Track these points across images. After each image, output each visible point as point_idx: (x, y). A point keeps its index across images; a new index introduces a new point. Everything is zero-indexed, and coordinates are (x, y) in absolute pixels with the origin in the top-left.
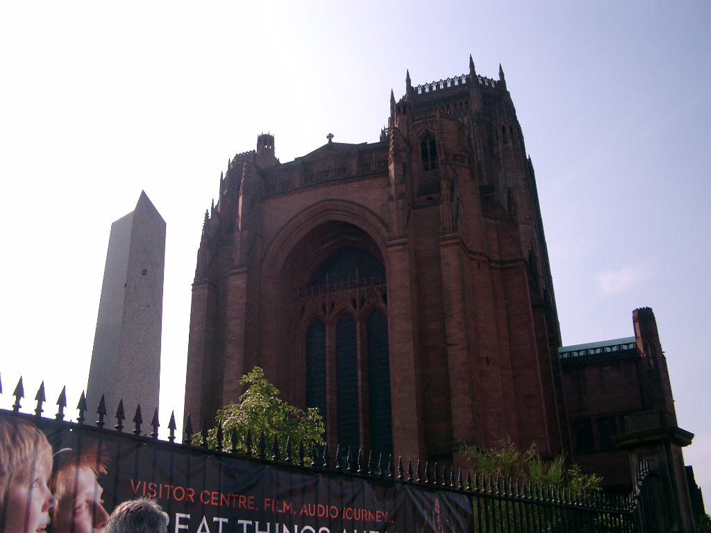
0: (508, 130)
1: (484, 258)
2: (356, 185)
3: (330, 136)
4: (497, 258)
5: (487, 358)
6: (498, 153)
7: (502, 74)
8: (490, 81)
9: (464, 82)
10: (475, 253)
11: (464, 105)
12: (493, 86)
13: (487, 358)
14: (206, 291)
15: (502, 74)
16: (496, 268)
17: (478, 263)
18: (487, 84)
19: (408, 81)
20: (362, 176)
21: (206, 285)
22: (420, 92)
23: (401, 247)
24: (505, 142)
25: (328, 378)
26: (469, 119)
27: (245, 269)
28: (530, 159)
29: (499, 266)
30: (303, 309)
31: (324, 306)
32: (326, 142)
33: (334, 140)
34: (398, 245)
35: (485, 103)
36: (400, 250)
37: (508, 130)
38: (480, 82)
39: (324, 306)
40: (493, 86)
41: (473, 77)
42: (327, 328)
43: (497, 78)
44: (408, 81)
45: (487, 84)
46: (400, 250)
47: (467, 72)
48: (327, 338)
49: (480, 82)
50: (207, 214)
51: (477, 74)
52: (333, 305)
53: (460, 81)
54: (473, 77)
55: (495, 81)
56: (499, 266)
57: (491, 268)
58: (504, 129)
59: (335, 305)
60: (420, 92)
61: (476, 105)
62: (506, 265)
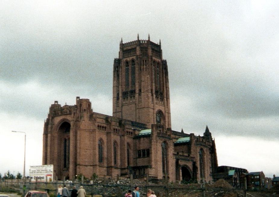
0: (145, 61)
3: (66, 103)
7: (149, 38)
8: (145, 41)
15: (149, 38)
18: (144, 42)
20: (69, 114)
24: (143, 66)
32: (65, 104)
33: (67, 104)
38: (141, 42)
40: (146, 42)
43: (147, 39)
44: (122, 41)
45: (144, 42)
51: (140, 39)
54: (139, 41)
58: (143, 61)
61: (138, 52)
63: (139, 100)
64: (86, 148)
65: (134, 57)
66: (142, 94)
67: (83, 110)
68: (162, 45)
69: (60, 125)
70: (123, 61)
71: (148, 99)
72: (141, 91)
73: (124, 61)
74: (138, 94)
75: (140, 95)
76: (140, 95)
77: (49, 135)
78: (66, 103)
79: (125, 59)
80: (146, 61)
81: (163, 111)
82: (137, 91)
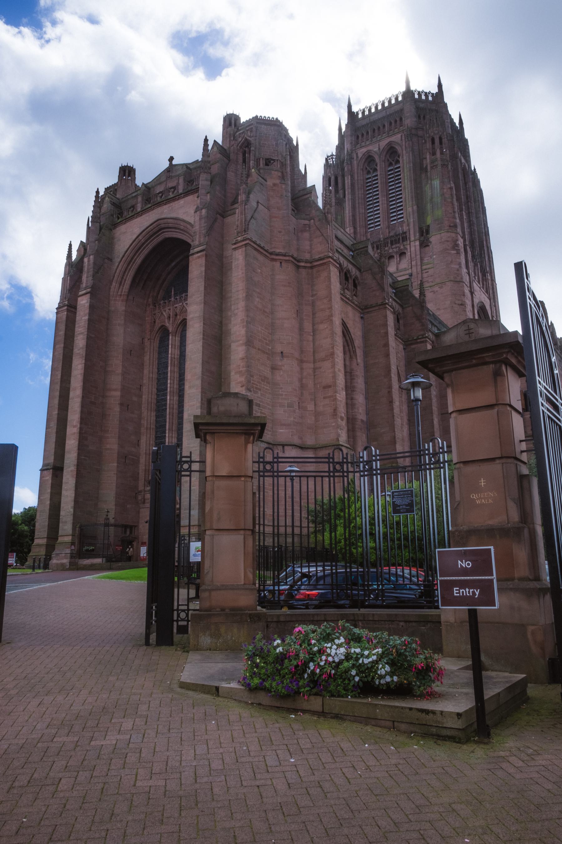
0: (437, 141)
1: (287, 258)
2: (182, 202)
3: (171, 159)
4: (307, 256)
5: (282, 352)
6: (427, 166)
7: (440, 86)
9: (400, 99)
10: (277, 255)
11: (398, 122)
12: (430, 98)
13: (282, 352)
14: (66, 313)
15: (440, 86)
16: (305, 267)
17: (281, 263)
18: (423, 97)
19: (350, 106)
20: (187, 193)
21: (66, 308)
22: (360, 116)
23: (199, 254)
24: (434, 154)
25: (169, 381)
26: (402, 136)
27: (89, 290)
28: (475, 169)
29: (309, 265)
30: (155, 322)
31: (169, 317)
32: (167, 165)
33: (174, 162)
34: (198, 252)
35: (419, 117)
36: (199, 257)
37: (437, 141)
38: (416, 96)
39: (169, 317)
40: (430, 98)
41: (408, 93)
42: (170, 337)
43: (435, 90)
44: (350, 106)
45: (423, 97)
46: (199, 257)
47: (403, 89)
48: (170, 346)
49: (416, 96)
50: (70, 246)
51: (413, 88)
52: (176, 315)
53: (397, 99)
55: (433, 94)
56: (309, 265)
57: (298, 267)
59: (178, 317)
60: (360, 116)
61: (409, 121)
62: (316, 264)
63: (422, 259)
64: (279, 348)
65: (396, 138)
66: (434, 239)
67: (257, 161)
68: (464, 126)
69: (139, 261)
70: (357, 157)
71: (458, 253)
72: (428, 232)
73: (360, 155)
74: (417, 243)
75: (424, 244)
76: (424, 244)
77: (84, 302)
78: (171, 159)
79: (361, 152)
80: (441, 139)
81: (488, 308)
82: (413, 235)
